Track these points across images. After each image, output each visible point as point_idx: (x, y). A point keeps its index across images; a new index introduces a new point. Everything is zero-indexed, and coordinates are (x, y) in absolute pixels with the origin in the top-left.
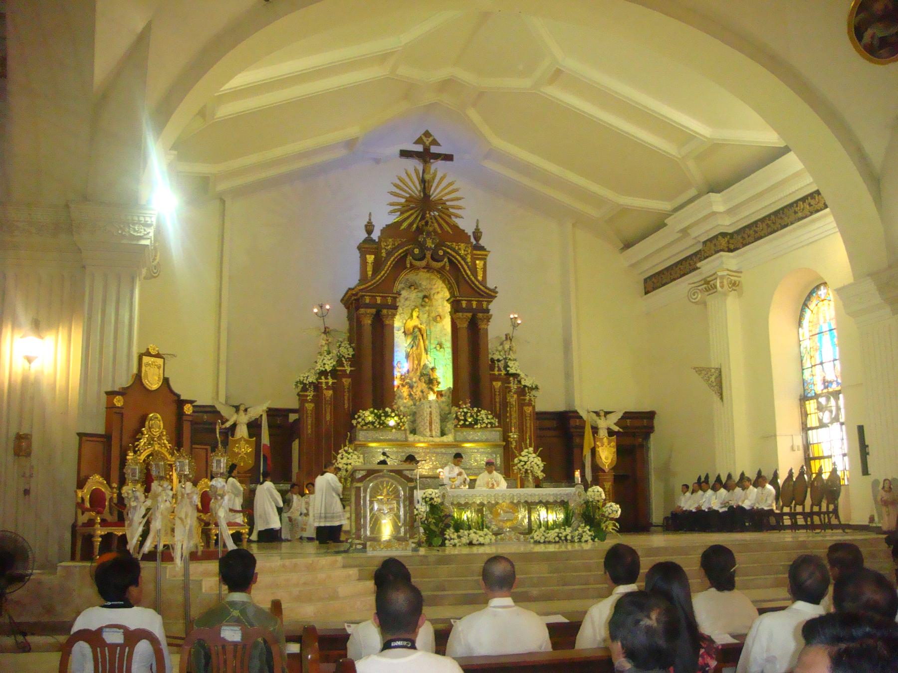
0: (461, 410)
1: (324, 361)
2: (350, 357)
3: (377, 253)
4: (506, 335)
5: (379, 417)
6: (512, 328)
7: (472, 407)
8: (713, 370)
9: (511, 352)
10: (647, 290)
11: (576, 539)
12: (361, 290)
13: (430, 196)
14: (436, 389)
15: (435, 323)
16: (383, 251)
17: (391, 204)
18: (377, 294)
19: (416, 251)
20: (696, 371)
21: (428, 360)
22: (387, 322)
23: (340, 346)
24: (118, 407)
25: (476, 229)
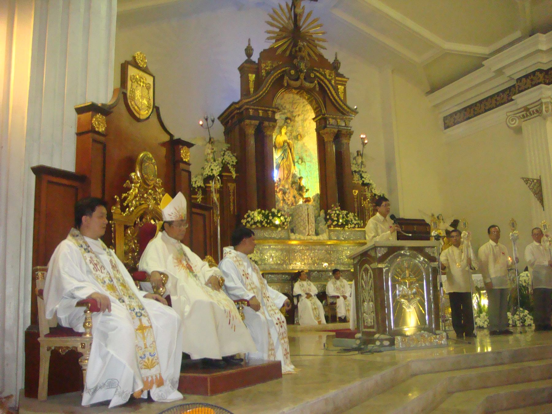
0: (334, 212)
1: (212, 167)
2: (235, 164)
3: (257, 72)
4: (358, 152)
5: (267, 217)
6: (362, 146)
7: (343, 209)
8: (535, 181)
9: (363, 166)
10: (446, 126)
11: (518, 324)
12: (247, 103)
13: (300, 28)
14: (305, 196)
15: (296, 141)
16: (263, 71)
17: (269, 32)
18: (260, 108)
19: (293, 72)
20: (524, 181)
21: (297, 170)
22: (268, 133)
23: (224, 155)
24: (98, 133)
25: (335, 60)
